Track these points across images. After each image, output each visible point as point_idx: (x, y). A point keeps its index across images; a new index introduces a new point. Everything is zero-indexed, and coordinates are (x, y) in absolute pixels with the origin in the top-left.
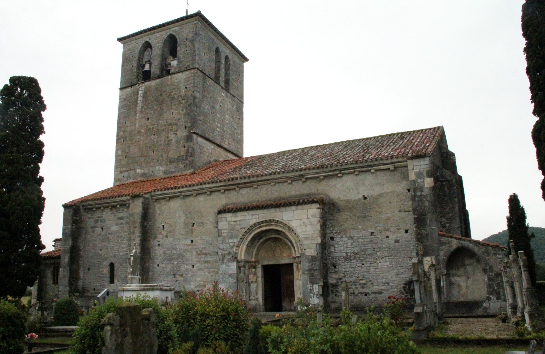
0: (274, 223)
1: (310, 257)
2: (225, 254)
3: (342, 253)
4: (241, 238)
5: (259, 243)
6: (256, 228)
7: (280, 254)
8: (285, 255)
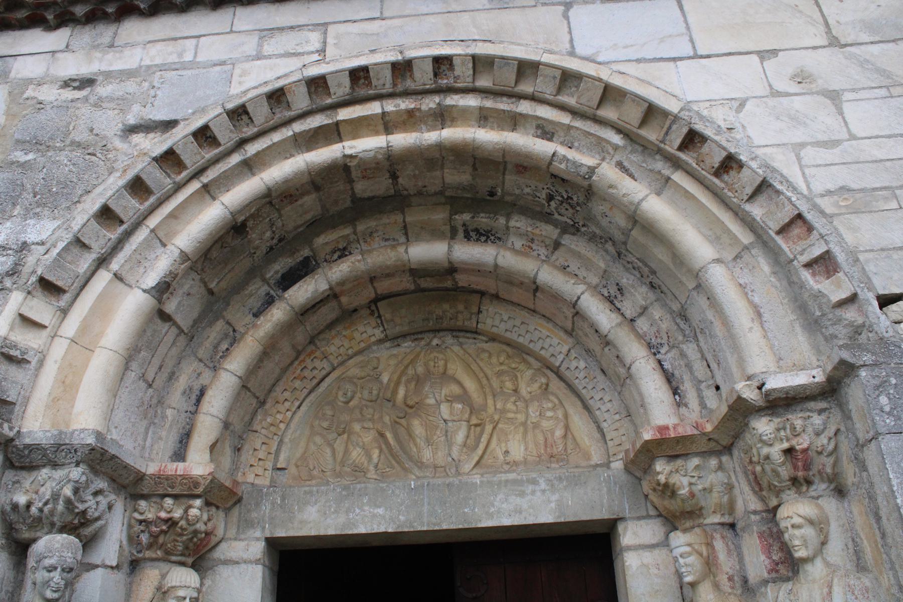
0: (472, 101)
4: (106, 214)
5: (278, 314)
6: (276, 137)
7: (469, 447)
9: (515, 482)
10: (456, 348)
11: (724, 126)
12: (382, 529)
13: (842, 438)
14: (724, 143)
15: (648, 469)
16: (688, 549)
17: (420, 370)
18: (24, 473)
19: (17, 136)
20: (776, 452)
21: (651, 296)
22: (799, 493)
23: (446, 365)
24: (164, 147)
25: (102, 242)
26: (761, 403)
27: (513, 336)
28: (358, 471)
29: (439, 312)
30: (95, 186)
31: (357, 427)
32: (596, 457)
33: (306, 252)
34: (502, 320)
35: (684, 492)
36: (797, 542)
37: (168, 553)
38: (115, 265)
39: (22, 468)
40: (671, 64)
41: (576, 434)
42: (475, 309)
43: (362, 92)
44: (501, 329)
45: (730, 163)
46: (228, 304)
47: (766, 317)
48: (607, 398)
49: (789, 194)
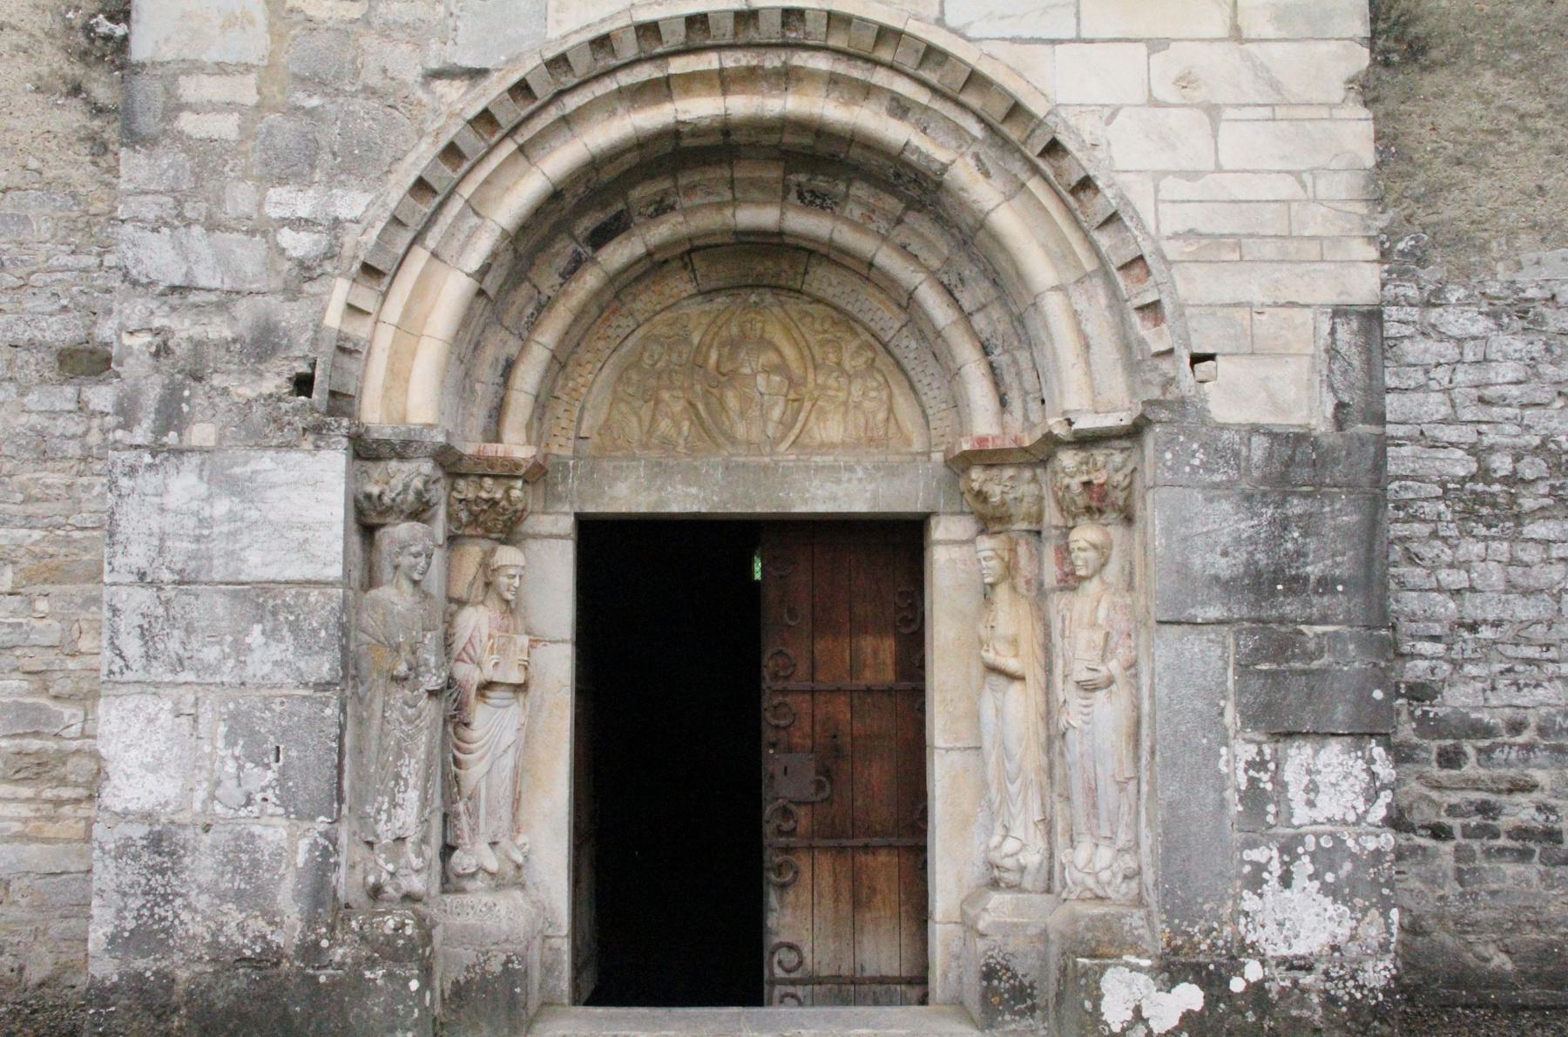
0: (820, 63)
1: (1259, 445)
2: (198, 346)
3: (1435, 445)
4: (421, 187)
5: (590, 280)
7: (786, 425)
8: (832, 429)
9: (834, 468)
10: (776, 310)
11: (1089, 140)
12: (695, 509)
13: (1137, 475)
14: (1085, 163)
15: (966, 471)
16: (990, 553)
17: (735, 330)
18: (369, 464)
19: (294, 68)
20: (1075, 483)
21: (993, 293)
22: (1091, 519)
23: (763, 329)
24: (477, 108)
25: (418, 217)
26: (1070, 439)
27: (842, 304)
28: (667, 444)
29: (760, 268)
30: (405, 153)
31: (665, 395)
32: (917, 446)
33: (620, 206)
34: (830, 284)
35: (995, 499)
36: (1079, 563)
37: (488, 530)
38: (432, 240)
39: (367, 459)
40: (1047, 49)
41: (899, 417)
42: (802, 270)
43: (698, 40)
44: (829, 292)
45: (1086, 184)
46: (533, 264)
47: (1094, 349)
48: (935, 385)
49: (1136, 233)
